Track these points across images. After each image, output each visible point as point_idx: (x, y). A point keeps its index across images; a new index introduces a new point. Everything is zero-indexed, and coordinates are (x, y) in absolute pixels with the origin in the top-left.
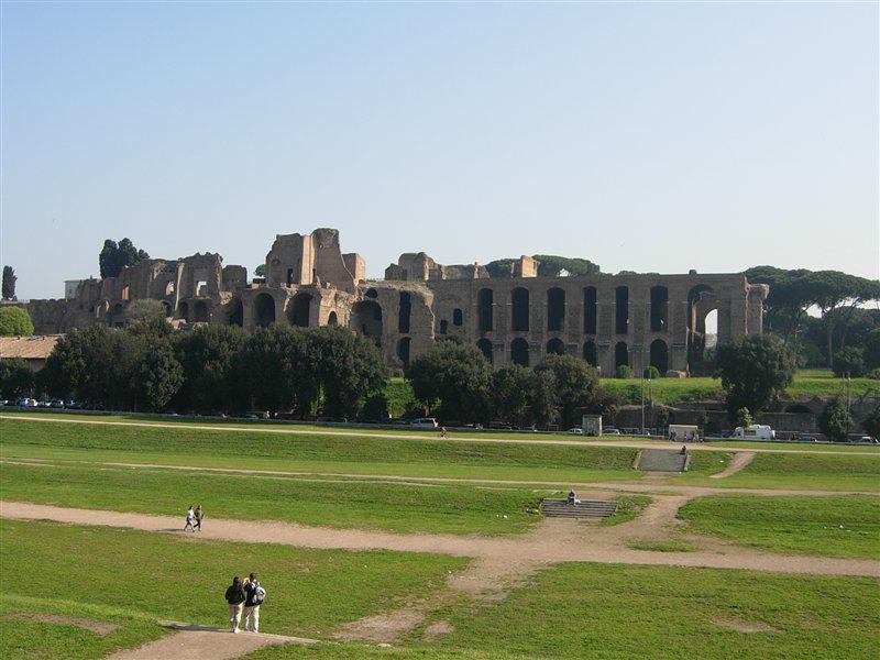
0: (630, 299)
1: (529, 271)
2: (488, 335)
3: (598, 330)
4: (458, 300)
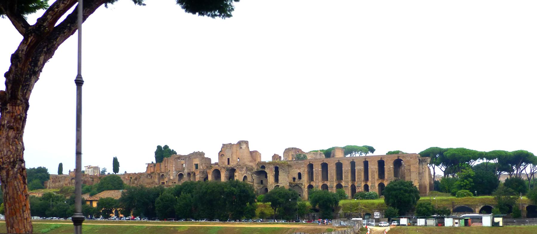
1: (339, 155)
2: (312, 183)
3: (356, 180)
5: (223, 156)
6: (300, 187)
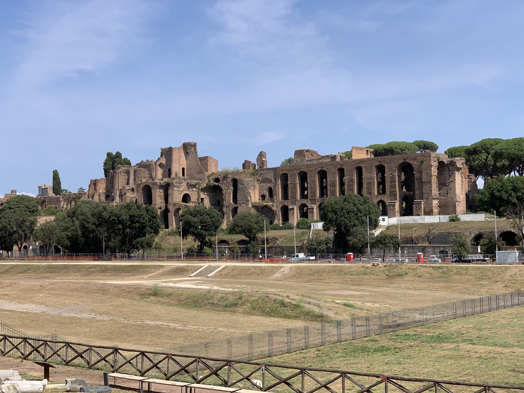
4: (270, 181)
5: (162, 165)
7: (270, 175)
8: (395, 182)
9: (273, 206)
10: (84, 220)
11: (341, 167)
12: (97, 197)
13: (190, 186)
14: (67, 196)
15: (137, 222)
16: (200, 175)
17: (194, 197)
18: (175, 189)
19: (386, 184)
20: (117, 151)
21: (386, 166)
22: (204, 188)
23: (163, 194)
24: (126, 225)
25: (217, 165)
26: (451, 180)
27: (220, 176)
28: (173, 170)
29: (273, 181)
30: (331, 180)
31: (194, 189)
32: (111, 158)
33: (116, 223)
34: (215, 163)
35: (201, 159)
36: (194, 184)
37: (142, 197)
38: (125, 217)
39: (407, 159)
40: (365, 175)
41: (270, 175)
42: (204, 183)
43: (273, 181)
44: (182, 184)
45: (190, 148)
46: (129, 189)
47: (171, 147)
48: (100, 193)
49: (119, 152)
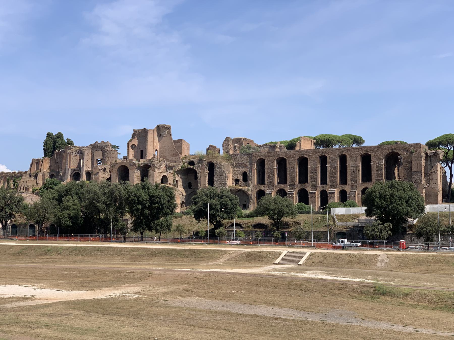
0: (348, 162)
1: (307, 146)
3: (328, 183)
4: (245, 166)
5: (134, 146)
6: (246, 193)
7: (245, 160)
8: (381, 170)
9: (248, 190)
10: (94, 199)
11: (323, 154)
12: (41, 176)
13: (168, 168)
14: (4, 175)
15: (157, 203)
16: (175, 157)
17: (170, 180)
18: (156, 170)
19: (372, 172)
20: (60, 132)
21: (372, 155)
22: (179, 170)
23: (139, 175)
24: (145, 206)
25: (188, 149)
26: (433, 170)
27: (194, 159)
28: (148, 152)
29: (249, 166)
30: (312, 167)
31: (171, 171)
32: (51, 138)
33: (135, 203)
34: (187, 147)
35: (176, 142)
36: (172, 166)
37: (117, 178)
38: (145, 197)
39: (395, 149)
40: (349, 163)
41: (245, 160)
42: (179, 165)
43: (249, 166)
44: (162, 165)
45: (164, 130)
46: (101, 169)
47: (145, 129)
48: (44, 172)
49: (61, 133)
